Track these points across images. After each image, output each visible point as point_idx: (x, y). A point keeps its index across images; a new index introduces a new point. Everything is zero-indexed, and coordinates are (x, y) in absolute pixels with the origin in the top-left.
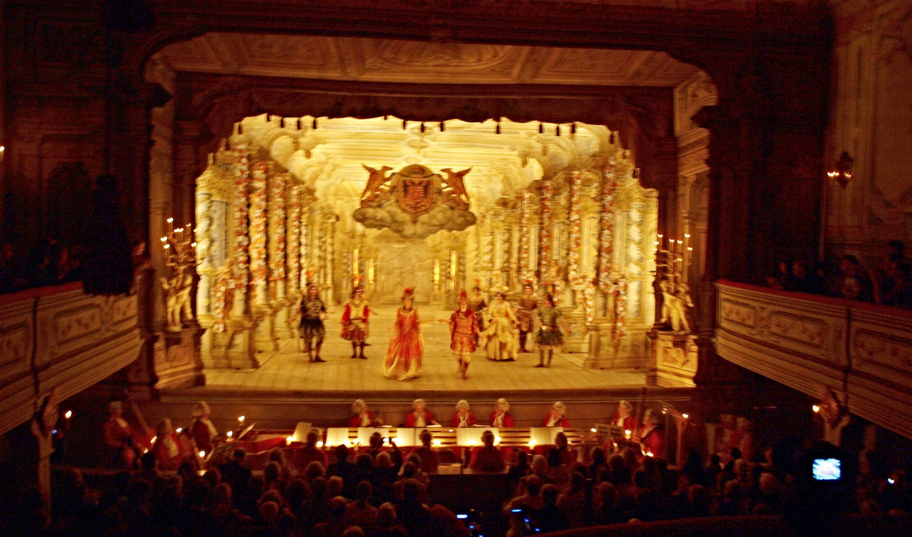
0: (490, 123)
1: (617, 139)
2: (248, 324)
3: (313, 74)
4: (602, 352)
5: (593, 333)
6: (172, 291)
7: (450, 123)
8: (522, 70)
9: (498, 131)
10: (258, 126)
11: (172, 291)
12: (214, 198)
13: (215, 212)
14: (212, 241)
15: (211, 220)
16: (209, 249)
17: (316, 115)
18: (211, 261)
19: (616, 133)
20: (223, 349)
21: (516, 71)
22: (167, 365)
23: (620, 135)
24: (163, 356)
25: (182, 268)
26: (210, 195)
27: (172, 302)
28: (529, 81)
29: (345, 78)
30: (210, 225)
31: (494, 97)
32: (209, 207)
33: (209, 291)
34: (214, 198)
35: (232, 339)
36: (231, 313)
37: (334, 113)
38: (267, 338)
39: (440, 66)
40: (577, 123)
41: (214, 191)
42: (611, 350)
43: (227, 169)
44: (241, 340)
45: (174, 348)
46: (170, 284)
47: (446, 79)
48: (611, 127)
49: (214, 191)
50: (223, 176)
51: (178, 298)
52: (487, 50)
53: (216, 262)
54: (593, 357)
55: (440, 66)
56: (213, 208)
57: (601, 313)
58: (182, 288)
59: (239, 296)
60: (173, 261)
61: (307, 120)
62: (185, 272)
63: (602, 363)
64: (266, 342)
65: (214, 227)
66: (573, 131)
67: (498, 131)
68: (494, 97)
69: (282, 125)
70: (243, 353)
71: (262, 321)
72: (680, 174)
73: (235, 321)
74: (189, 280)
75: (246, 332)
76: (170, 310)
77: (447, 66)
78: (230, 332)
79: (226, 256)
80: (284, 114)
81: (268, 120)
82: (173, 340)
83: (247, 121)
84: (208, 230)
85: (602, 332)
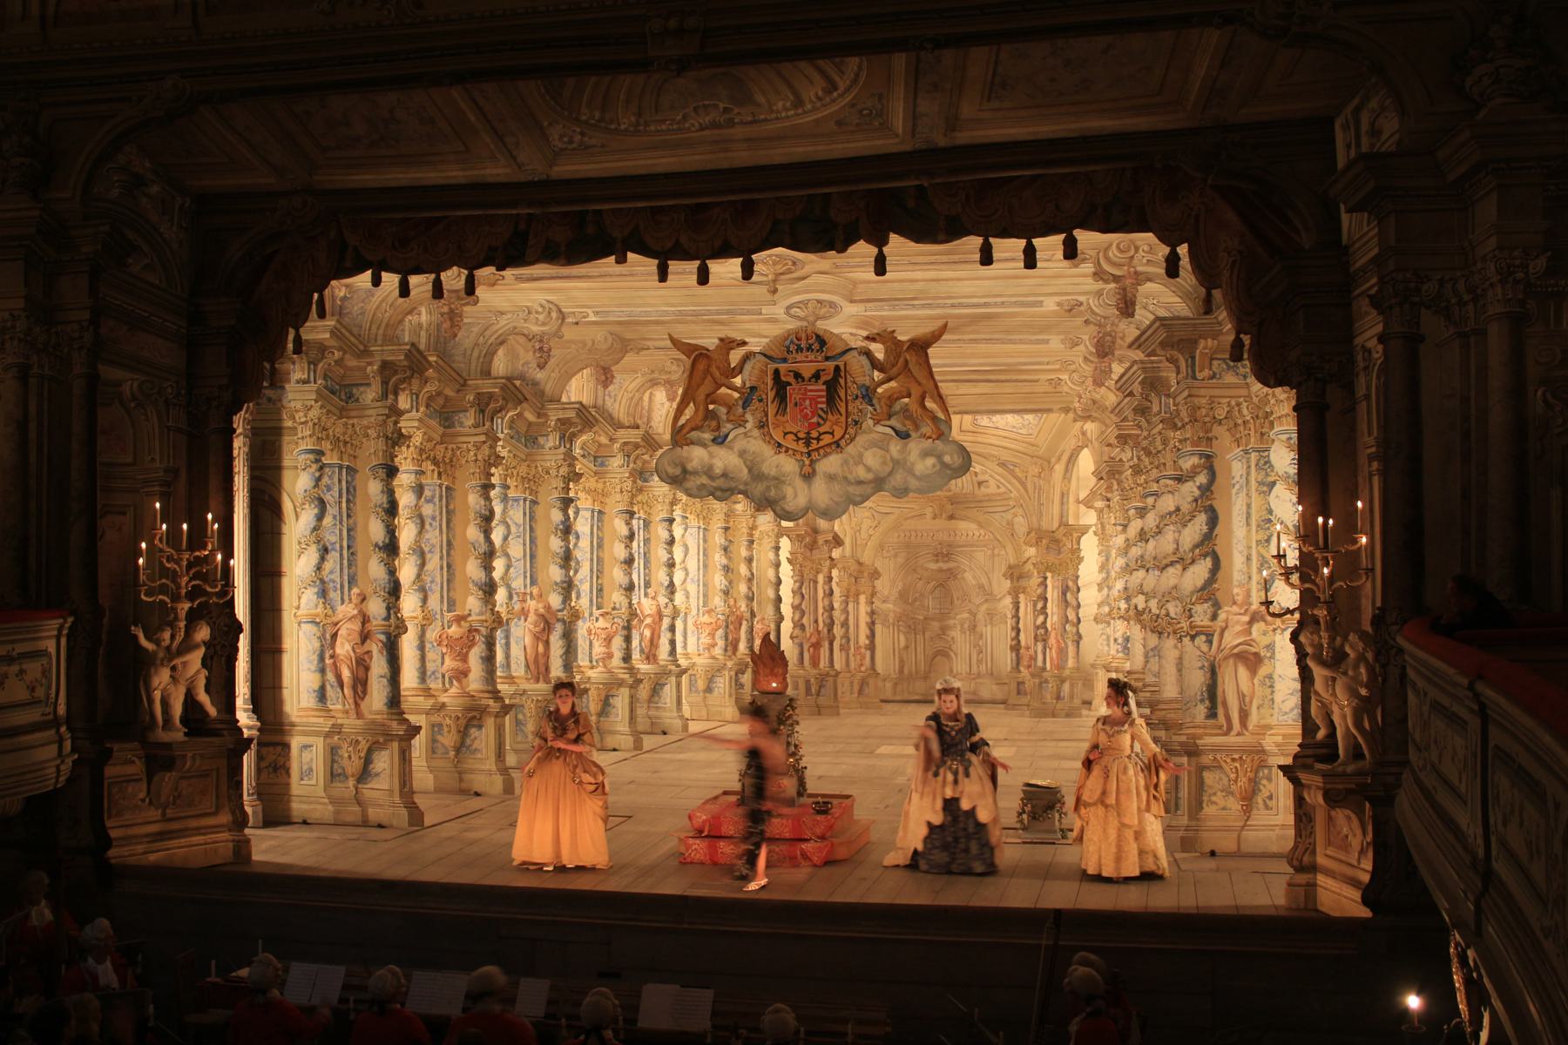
0: (863, 251)
1: (1185, 262)
2: (398, 729)
3: (453, 174)
4: (1209, 810)
5: (1185, 759)
6: (161, 655)
7: (768, 260)
8: (914, 117)
9: (880, 267)
10: (365, 295)
11: (161, 655)
12: (325, 460)
13: (329, 488)
14: (325, 551)
15: (322, 504)
16: (319, 568)
17: (472, 266)
18: (323, 594)
19: (1183, 250)
20: (351, 782)
21: (899, 122)
22: (155, 814)
23: (1192, 253)
24: (142, 795)
25: (186, 606)
26: (320, 453)
27: (161, 678)
28: (942, 142)
29: (522, 178)
30: (320, 517)
31: (862, 187)
32: (319, 479)
33: (322, 658)
34: (325, 460)
35: (368, 761)
36: (363, 705)
37: (511, 254)
38: (491, 764)
39: (715, 125)
40: (1077, 233)
41: (326, 446)
42: (1234, 805)
43: (350, 396)
44: (384, 762)
45: (168, 779)
46: (158, 643)
47: (742, 157)
48: (1168, 237)
49: (326, 446)
50: (343, 413)
51: (174, 669)
52: (809, 81)
53: (334, 595)
54: (1184, 821)
55: (715, 125)
56: (325, 480)
57: (1201, 711)
58: (187, 647)
59: (379, 666)
60: (163, 589)
61: (453, 278)
62: (193, 617)
63: (1211, 840)
64: (490, 773)
65: (328, 520)
66: (1071, 252)
67: (880, 267)
68: (862, 187)
69: (404, 291)
70: (391, 791)
71: (480, 727)
72: (1358, 341)
73: (373, 722)
74: (203, 633)
75: (395, 745)
76: (157, 695)
77: (731, 123)
78: (364, 746)
79: (352, 581)
80: (405, 273)
81: (376, 281)
82: (159, 760)
83: (338, 289)
84: (315, 529)
85: (1206, 759)
